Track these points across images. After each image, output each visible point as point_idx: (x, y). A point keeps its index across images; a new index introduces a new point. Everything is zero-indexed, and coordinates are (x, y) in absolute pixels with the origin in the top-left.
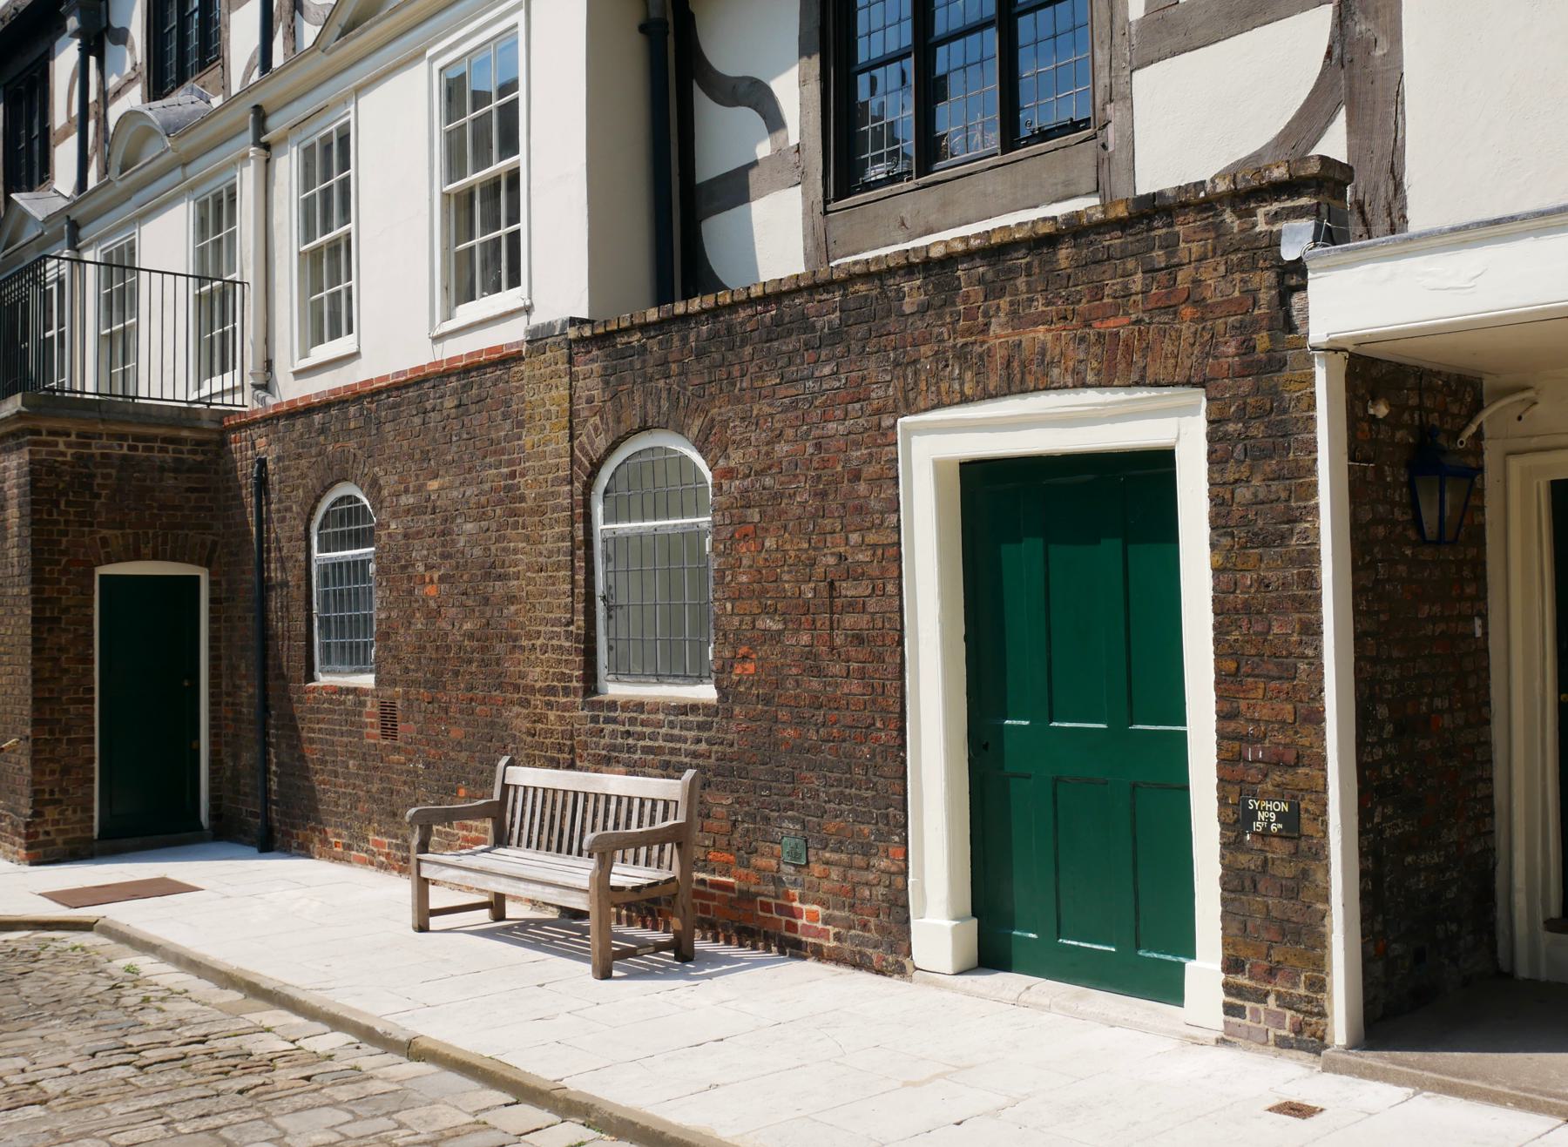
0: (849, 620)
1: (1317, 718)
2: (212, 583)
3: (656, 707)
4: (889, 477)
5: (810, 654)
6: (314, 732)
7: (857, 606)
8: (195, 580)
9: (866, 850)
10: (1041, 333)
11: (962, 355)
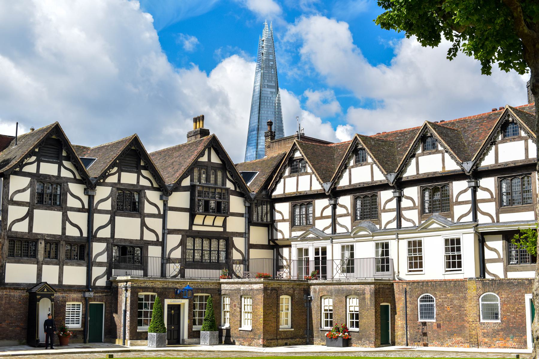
0: (519, 314)
2: (391, 306)
3: (491, 323)
5: (514, 317)
7: (519, 312)
8: (388, 305)
9: (522, 337)
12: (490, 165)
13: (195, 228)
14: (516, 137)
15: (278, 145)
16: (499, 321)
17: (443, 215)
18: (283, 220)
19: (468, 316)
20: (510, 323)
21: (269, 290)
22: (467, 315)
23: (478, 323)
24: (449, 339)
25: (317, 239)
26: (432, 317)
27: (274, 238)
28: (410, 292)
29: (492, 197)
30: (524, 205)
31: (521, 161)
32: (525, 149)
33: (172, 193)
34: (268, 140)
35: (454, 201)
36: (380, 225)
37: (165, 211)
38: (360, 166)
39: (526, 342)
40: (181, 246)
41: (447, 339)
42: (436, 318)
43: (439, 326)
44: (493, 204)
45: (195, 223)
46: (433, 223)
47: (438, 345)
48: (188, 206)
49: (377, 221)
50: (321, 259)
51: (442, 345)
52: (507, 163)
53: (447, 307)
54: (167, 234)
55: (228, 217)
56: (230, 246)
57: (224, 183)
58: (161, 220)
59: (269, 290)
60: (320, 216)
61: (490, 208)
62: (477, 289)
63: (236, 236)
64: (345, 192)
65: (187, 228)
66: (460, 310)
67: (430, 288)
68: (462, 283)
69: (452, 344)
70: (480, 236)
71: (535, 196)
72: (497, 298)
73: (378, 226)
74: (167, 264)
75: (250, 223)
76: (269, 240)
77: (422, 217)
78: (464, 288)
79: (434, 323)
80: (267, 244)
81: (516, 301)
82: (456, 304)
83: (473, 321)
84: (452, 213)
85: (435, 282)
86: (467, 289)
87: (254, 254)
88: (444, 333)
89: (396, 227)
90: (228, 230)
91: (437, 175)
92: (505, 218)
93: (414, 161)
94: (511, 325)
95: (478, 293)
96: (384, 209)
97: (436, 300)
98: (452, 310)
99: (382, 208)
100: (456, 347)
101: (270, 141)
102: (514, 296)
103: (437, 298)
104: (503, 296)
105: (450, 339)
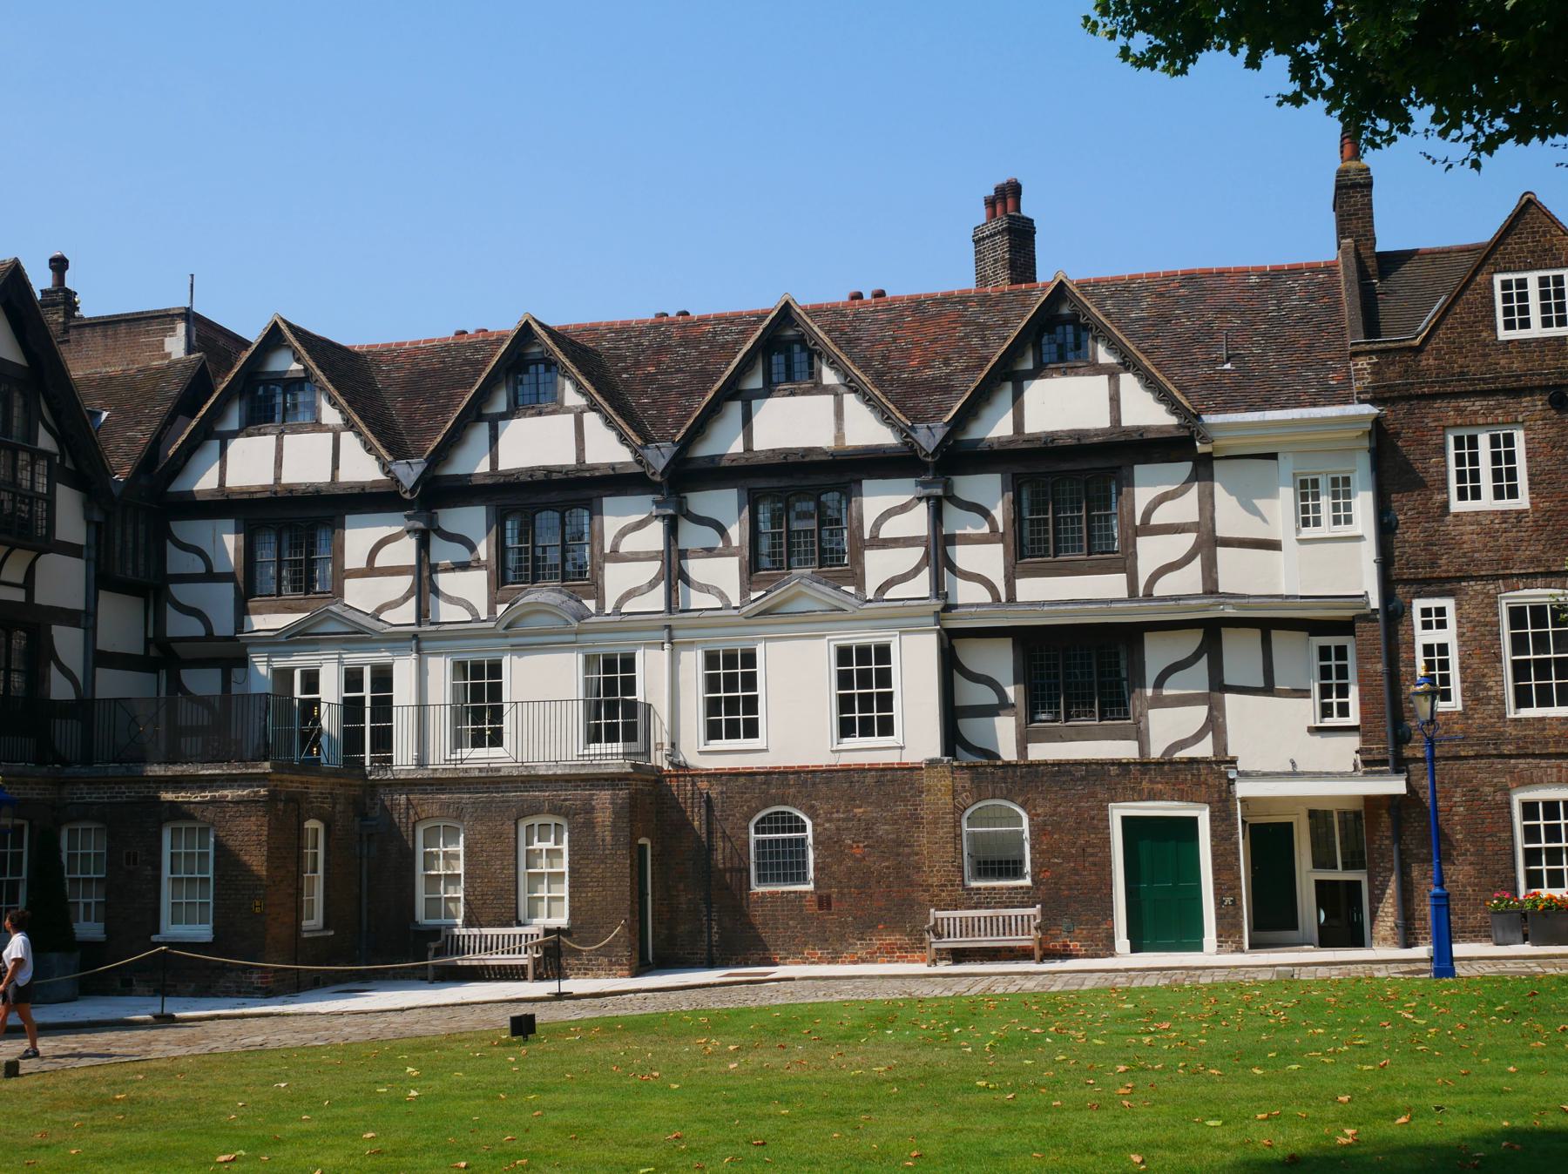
0: (1091, 859)
1: (1240, 878)
2: (652, 847)
3: (1002, 888)
4: (1106, 819)
5: (1074, 869)
6: (757, 915)
7: (1092, 855)
9: (1098, 924)
10: (1160, 786)
11: (1133, 789)
12: (999, 438)
14: (1080, 364)
15: (106, 336)
16: (1027, 882)
17: (830, 575)
18: (211, 576)
19: (925, 872)
20: (1063, 887)
21: (281, 800)
22: (919, 868)
23: (960, 888)
24: (859, 940)
26: (802, 878)
27: (169, 634)
28: (723, 803)
29: (994, 529)
30: (824, 569)
31: (1097, 432)
32: (1111, 399)
34: (55, 317)
35: (867, 536)
36: (600, 597)
38: (532, 415)
39: (1110, 938)
41: (851, 941)
42: (816, 881)
43: (824, 902)
44: (998, 549)
46: (800, 595)
47: (819, 958)
49: (586, 588)
50: (368, 703)
51: (833, 960)
52: (1052, 436)
53: (855, 846)
56: (41, 654)
57: (31, 437)
59: (281, 800)
61: (985, 559)
62: (955, 793)
63: (61, 623)
64: (719, 474)
66: (898, 855)
67: (792, 791)
68: (904, 776)
69: (867, 953)
70: (946, 638)
71: (1130, 531)
72: (1020, 817)
73: (591, 604)
75: (102, 579)
76: (147, 642)
77: (754, 578)
78: (910, 788)
79: (808, 896)
80: (141, 653)
81: (1080, 823)
82: (884, 837)
83: (942, 885)
84: (858, 571)
85: (813, 772)
86: (922, 792)
87: (110, 684)
88: (843, 925)
89: (662, 608)
90: (43, 597)
91: (815, 458)
92: (1031, 589)
93: (735, 409)
94: (1066, 892)
95: (959, 802)
96: (615, 550)
97: (814, 825)
98: (869, 855)
99: (607, 550)
100: (883, 962)
101: (61, 320)
102: (1073, 810)
103: (819, 820)
104: (1039, 811)
105: (865, 940)
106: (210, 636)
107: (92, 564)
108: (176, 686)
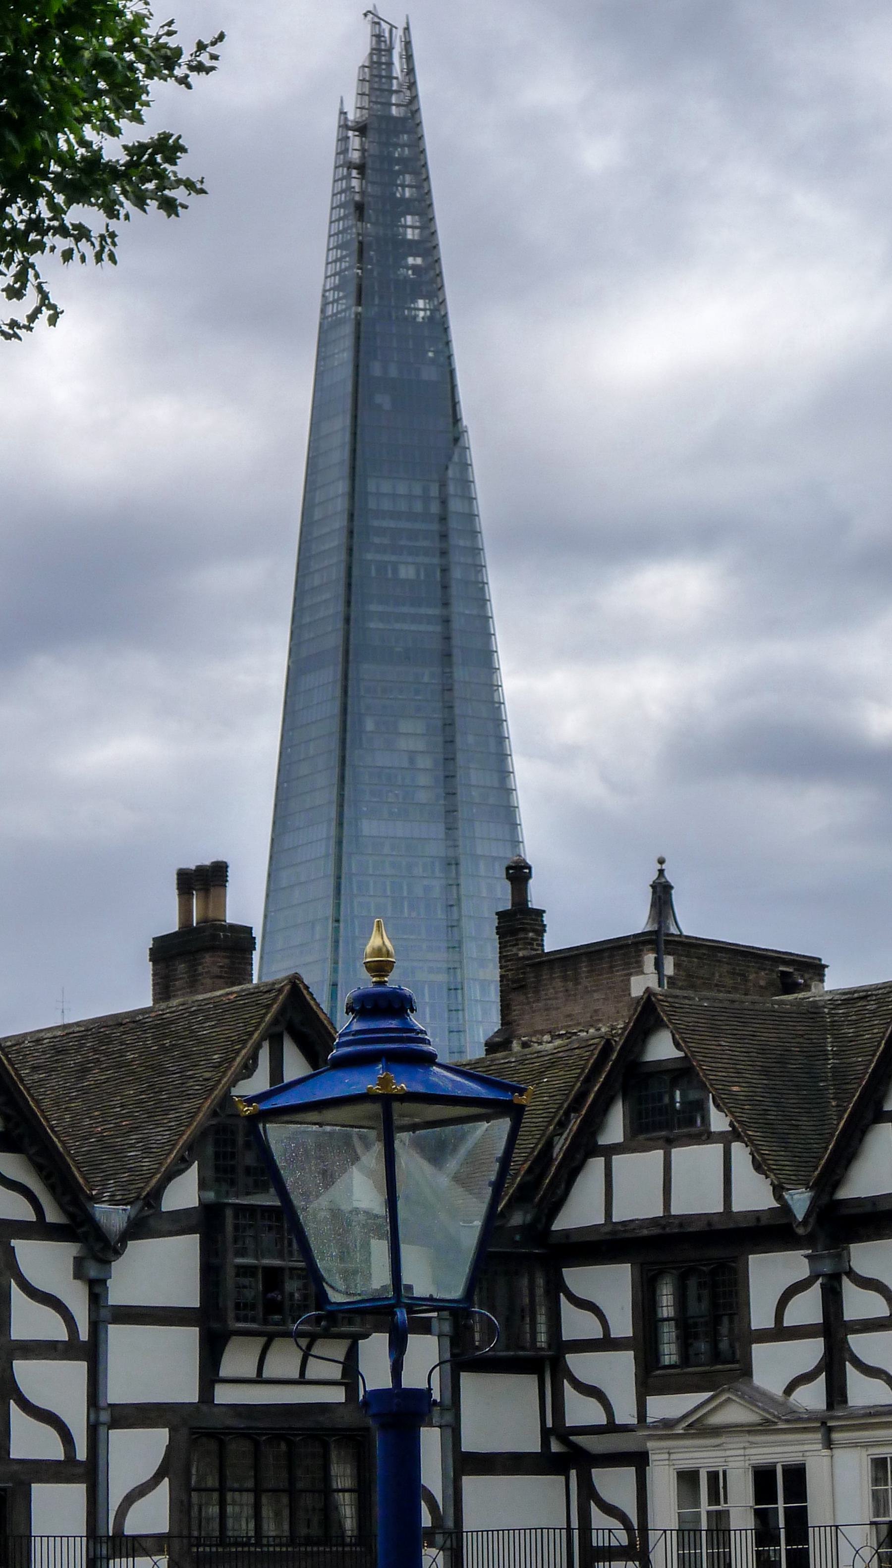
13: (224, 1395)
15: (565, 978)
18: (607, 1343)
25: (765, 1427)
33: (124, 1246)
34: (515, 950)
37: (95, 1327)
40: (166, 1480)
45: (224, 1372)
48: (192, 1299)
54: (109, 1429)
55: (366, 1336)
58: (81, 1367)
60: (771, 1324)
65: (190, 1394)
74: (111, 1562)
76: (546, 1434)
106: (611, 1428)
107: (447, 1342)
108: (588, 1492)
